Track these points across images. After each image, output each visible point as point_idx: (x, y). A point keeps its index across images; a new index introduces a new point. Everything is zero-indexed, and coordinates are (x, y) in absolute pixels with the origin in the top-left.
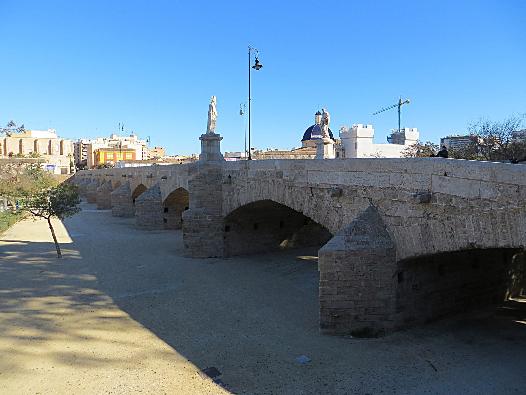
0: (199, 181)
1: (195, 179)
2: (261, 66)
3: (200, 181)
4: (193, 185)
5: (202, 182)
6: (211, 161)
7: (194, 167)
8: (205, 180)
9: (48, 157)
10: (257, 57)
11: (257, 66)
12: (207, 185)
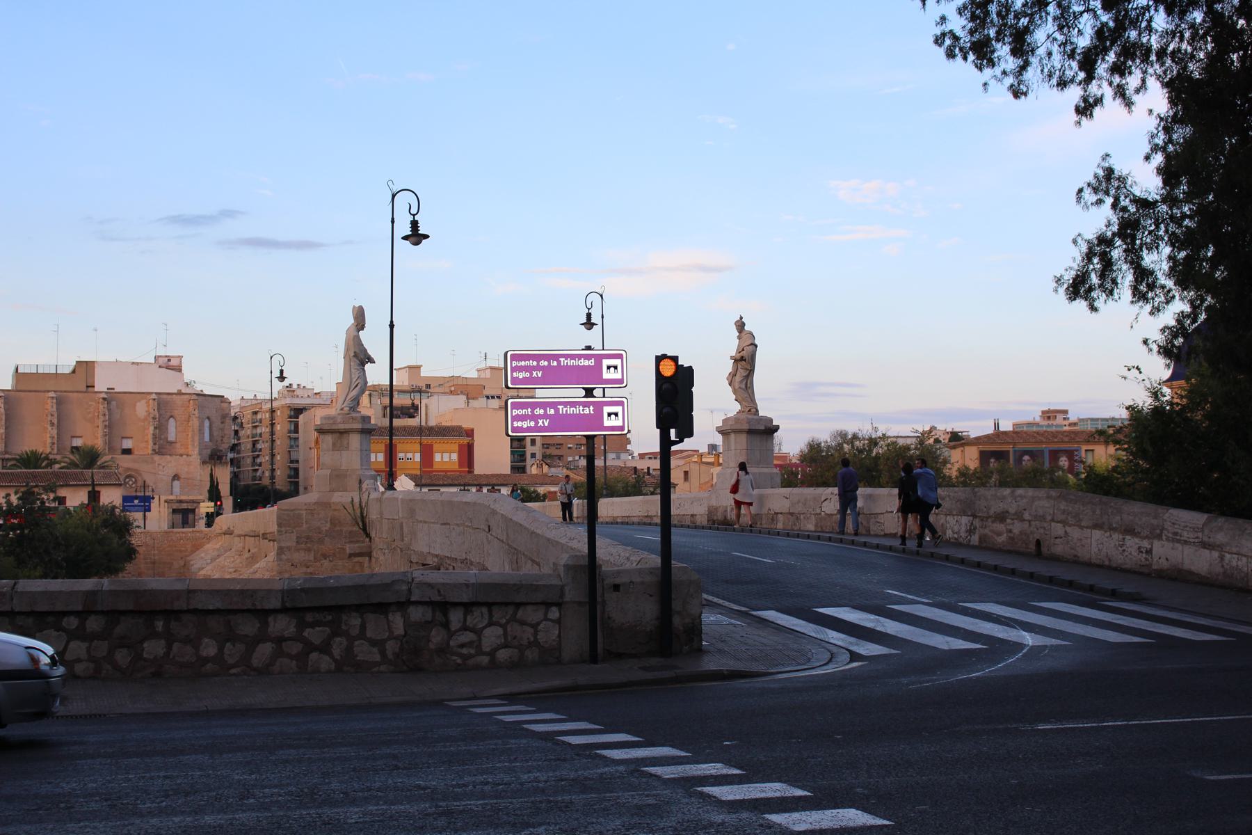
0: (305, 550)
1: (294, 544)
2: (426, 237)
3: (309, 550)
4: (288, 560)
5: (313, 555)
6: (340, 493)
7: (292, 510)
8: (320, 547)
9: (136, 466)
10: (414, 211)
11: (416, 236)
12: (326, 563)
